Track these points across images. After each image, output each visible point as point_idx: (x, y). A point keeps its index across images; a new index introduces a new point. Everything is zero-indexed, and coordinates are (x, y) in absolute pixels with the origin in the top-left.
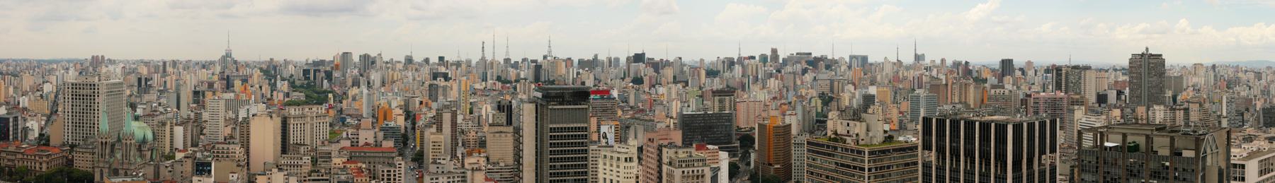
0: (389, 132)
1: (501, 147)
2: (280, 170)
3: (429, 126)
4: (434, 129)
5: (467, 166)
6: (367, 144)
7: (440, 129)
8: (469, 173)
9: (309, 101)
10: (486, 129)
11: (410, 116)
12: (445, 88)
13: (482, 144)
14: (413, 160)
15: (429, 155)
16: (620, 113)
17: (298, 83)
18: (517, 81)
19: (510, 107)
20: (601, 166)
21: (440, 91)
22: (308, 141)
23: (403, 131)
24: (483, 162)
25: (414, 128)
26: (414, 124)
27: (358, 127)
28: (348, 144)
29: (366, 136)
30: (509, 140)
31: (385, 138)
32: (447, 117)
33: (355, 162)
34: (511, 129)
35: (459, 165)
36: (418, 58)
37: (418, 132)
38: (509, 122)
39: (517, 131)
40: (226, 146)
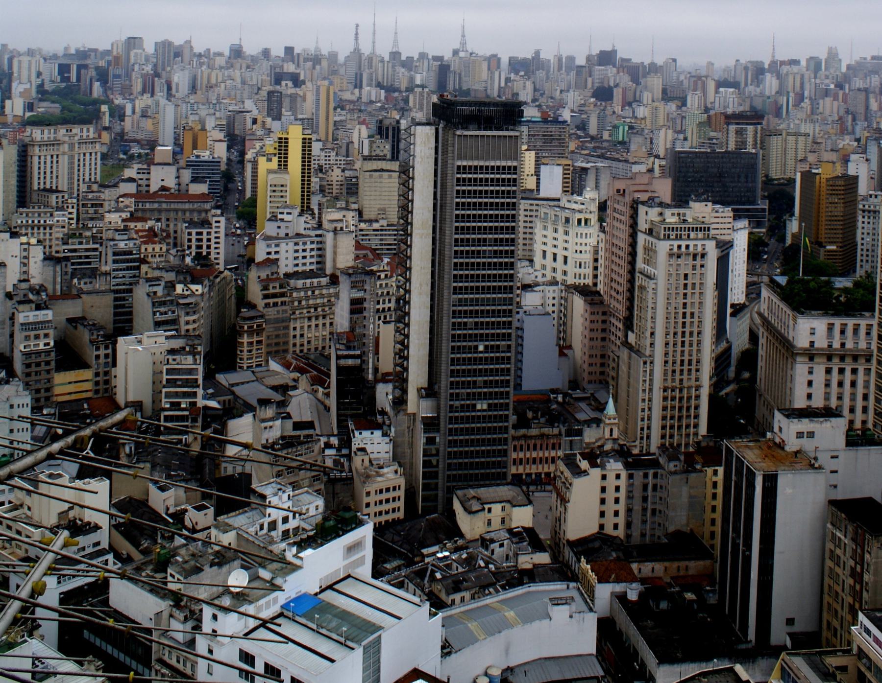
0: (201, 170)
1: (379, 193)
5: (326, 225)
6: (163, 188)
7: (283, 165)
8: (329, 237)
9: (67, 120)
10: (357, 165)
11: (236, 141)
12: (293, 98)
13: (352, 188)
14: (240, 217)
17: (48, 87)
18: (410, 89)
19: (397, 130)
21: (286, 102)
22: (63, 185)
23: (223, 167)
24: (351, 218)
25: (242, 162)
26: (243, 154)
27: (149, 161)
28: (131, 188)
29: (162, 177)
30: (392, 183)
31: (195, 180)
33: (144, 220)
34: (395, 166)
35: (313, 223)
38: (395, 157)
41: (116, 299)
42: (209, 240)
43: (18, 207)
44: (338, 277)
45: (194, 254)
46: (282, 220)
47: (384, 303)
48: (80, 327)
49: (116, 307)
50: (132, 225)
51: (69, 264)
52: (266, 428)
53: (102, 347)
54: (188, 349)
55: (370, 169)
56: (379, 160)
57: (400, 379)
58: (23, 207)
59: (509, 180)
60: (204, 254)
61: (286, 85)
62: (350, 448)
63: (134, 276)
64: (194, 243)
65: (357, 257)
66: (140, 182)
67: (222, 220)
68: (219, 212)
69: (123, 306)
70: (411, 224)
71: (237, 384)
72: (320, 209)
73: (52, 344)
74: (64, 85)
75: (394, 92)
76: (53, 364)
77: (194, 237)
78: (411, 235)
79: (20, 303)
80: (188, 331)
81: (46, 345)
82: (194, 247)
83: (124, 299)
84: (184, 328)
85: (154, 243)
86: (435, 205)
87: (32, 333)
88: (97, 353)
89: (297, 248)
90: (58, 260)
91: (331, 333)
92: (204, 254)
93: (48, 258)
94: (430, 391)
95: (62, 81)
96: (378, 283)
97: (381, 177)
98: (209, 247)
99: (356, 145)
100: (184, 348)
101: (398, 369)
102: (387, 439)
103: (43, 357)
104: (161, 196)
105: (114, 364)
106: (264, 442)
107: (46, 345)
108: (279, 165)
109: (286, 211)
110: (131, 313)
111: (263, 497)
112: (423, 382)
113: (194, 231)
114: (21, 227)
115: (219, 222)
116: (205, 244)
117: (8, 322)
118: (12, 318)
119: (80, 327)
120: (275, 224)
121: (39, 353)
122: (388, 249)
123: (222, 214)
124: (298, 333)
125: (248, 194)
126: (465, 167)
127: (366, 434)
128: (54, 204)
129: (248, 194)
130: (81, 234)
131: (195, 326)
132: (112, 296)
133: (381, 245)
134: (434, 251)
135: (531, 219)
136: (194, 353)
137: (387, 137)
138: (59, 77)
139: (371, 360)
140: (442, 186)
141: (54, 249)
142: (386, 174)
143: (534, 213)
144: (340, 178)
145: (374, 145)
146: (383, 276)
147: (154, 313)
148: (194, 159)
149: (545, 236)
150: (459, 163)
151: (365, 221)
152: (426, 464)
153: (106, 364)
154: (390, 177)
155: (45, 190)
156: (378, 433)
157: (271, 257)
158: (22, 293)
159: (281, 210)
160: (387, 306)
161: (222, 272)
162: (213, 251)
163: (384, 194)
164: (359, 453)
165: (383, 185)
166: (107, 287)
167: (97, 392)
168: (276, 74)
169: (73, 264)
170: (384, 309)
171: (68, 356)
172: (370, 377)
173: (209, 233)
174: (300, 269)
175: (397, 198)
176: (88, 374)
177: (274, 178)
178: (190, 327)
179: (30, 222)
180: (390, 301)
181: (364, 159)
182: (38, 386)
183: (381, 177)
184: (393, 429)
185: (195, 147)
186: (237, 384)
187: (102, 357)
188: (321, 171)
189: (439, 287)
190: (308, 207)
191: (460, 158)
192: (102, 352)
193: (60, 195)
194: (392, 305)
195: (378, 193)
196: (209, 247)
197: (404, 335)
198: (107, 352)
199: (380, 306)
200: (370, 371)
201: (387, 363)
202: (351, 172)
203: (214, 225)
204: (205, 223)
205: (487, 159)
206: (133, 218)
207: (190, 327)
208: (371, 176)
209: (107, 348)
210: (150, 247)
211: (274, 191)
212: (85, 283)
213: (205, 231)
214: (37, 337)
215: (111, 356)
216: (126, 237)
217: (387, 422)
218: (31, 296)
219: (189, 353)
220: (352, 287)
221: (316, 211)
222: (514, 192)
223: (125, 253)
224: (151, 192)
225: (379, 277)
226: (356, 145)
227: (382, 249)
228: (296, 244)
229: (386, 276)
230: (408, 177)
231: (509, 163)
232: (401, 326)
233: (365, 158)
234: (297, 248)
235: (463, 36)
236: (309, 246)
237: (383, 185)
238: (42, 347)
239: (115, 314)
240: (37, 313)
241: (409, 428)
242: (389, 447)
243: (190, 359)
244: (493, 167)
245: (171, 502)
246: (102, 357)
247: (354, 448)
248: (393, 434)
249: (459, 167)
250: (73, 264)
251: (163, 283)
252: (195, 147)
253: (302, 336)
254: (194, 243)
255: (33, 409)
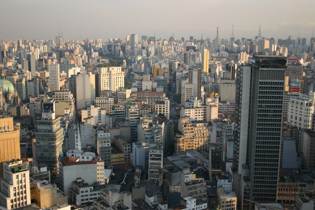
2: (95, 107)
3: (185, 78)
4: (187, 81)
7: (191, 81)
10: (219, 81)
13: (217, 90)
15: (185, 97)
16: (304, 74)
20: (290, 107)
25: (175, 81)
32: (195, 74)
34: (234, 81)
36: (177, 38)
37: (177, 83)
39: (239, 83)
40: (61, 93)
41: (131, 129)
42: (164, 109)
43: (96, 97)
44: (211, 123)
45: (158, 114)
46: (191, 102)
47: (229, 133)
48: (119, 139)
49: (131, 132)
50: (136, 103)
51: (115, 117)
52: (186, 177)
53: (127, 146)
54: (157, 147)
55: (225, 82)
56: (227, 79)
57: (235, 161)
58: (98, 97)
59: (280, 87)
60: (162, 114)
61: (191, 51)
62: (216, 186)
63: (138, 121)
64: (158, 110)
65: (219, 115)
66: (139, 88)
67: (169, 101)
68: (167, 98)
69: (134, 132)
70: (241, 104)
71: (175, 161)
72: (204, 98)
73: (110, 145)
74: (109, 53)
75: (232, 53)
76: (111, 151)
77: (158, 107)
78: (241, 108)
79: (98, 130)
80: (157, 141)
81: (108, 145)
82: (158, 111)
83: (134, 129)
84: (156, 140)
85: (144, 109)
86: (250, 97)
87: (103, 141)
88: (126, 148)
89: (196, 112)
90: (111, 115)
91: (209, 144)
92: (162, 114)
93: (107, 114)
94: (247, 165)
95: (109, 51)
96: (227, 125)
97: (228, 86)
98: (164, 111)
99: (218, 74)
100: (156, 147)
101: (235, 157)
102: (230, 183)
103: (107, 149)
104: (146, 93)
105: (132, 152)
106: (185, 182)
107: (108, 145)
108: (189, 81)
109: (192, 98)
110: (137, 134)
111: (186, 201)
112: (244, 162)
113: (158, 105)
114: (98, 104)
115: (167, 102)
116: (162, 110)
117: (95, 137)
118: (96, 135)
119: (119, 139)
120: (189, 103)
121: (106, 148)
122: (230, 113)
123: (168, 100)
124: (197, 143)
125: (177, 92)
126: (262, 82)
127: (222, 181)
128: (108, 96)
129: (177, 92)
130: (119, 106)
131: (160, 139)
132: (130, 128)
133: (228, 111)
134: (249, 114)
135: (287, 103)
136: (160, 149)
137: (230, 71)
138: (108, 50)
139: (224, 154)
140: (253, 89)
141: (109, 111)
142: (229, 85)
143: (288, 101)
144: (212, 86)
145: (225, 74)
146: (228, 123)
147: (145, 135)
148: (157, 79)
149: (292, 110)
150: (260, 81)
151: (222, 102)
152: (245, 193)
153: (129, 152)
154: (231, 86)
155: (105, 90)
156: (227, 181)
157: (187, 115)
158: (99, 127)
159: (191, 98)
160: (230, 134)
161: (169, 120)
162: (165, 113)
163: (229, 92)
164: (220, 187)
165: (229, 89)
166: (128, 125)
167: (126, 161)
168: (187, 47)
169: (116, 117)
170: (229, 135)
171: (115, 148)
172: (224, 160)
173: (164, 106)
174: (198, 120)
175: (235, 94)
176: (122, 155)
177: (187, 86)
178: (158, 140)
179: (101, 102)
180: (231, 132)
181: (222, 79)
182: (106, 159)
183: (228, 86)
184: (232, 180)
185: (158, 75)
186: (175, 161)
187: (127, 149)
188: (205, 83)
189: (251, 127)
190: (200, 97)
191: (261, 79)
192: (127, 148)
193: (110, 92)
194: (232, 134)
195: (227, 92)
196: (164, 111)
197: (237, 145)
198: (129, 148)
199: (228, 134)
200: (224, 158)
201: (230, 155)
202: (216, 84)
203: (166, 103)
204: (163, 103)
205: (272, 79)
206: (136, 101)
207: (158, 140)
208: (224, 85)
209: (129, 146)
210: (143, 111)
211: (187, 91)
212: (121, 124)
213: (162, 105)
214: (105, 142)
215: (130, 149)
216: (134, 107)
217: (230, 177)
218: (102, 128)
219: (158, 149)
220: (217, 127)
221: (203, 99)
222: (282, 92)
223: (134, 113)
224: (143, 91)
225: (227, 123)
226: (218, 74)
227: (228, 113)
228: (197, 110)
229: (230, 123)
230: (240, 86)
231: (280, 81)
232: (236, 142)
233: (222, 79)
234: (196, 112)
235: (260, 31)
236: (201, 111)
237: (229, 89)
238: (107, 145)
239: (131, 135)
240: (105, 134)
241: (238, 179)
242: (231, 186)
243: (158, 151)
244: (274, 83)
245: (152, 201)
246: (127, 149)
247: (218, 186)
248: (232, 181)
249: (260, 82)
250: (116, 117)
251: (148, 124)
252: (158, 75)
253: (198, 144)
254: (158, 110)
255: (105, 167)
